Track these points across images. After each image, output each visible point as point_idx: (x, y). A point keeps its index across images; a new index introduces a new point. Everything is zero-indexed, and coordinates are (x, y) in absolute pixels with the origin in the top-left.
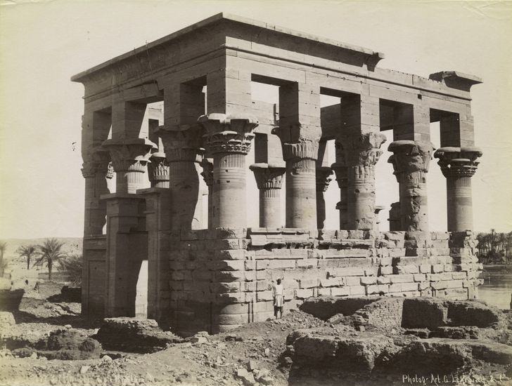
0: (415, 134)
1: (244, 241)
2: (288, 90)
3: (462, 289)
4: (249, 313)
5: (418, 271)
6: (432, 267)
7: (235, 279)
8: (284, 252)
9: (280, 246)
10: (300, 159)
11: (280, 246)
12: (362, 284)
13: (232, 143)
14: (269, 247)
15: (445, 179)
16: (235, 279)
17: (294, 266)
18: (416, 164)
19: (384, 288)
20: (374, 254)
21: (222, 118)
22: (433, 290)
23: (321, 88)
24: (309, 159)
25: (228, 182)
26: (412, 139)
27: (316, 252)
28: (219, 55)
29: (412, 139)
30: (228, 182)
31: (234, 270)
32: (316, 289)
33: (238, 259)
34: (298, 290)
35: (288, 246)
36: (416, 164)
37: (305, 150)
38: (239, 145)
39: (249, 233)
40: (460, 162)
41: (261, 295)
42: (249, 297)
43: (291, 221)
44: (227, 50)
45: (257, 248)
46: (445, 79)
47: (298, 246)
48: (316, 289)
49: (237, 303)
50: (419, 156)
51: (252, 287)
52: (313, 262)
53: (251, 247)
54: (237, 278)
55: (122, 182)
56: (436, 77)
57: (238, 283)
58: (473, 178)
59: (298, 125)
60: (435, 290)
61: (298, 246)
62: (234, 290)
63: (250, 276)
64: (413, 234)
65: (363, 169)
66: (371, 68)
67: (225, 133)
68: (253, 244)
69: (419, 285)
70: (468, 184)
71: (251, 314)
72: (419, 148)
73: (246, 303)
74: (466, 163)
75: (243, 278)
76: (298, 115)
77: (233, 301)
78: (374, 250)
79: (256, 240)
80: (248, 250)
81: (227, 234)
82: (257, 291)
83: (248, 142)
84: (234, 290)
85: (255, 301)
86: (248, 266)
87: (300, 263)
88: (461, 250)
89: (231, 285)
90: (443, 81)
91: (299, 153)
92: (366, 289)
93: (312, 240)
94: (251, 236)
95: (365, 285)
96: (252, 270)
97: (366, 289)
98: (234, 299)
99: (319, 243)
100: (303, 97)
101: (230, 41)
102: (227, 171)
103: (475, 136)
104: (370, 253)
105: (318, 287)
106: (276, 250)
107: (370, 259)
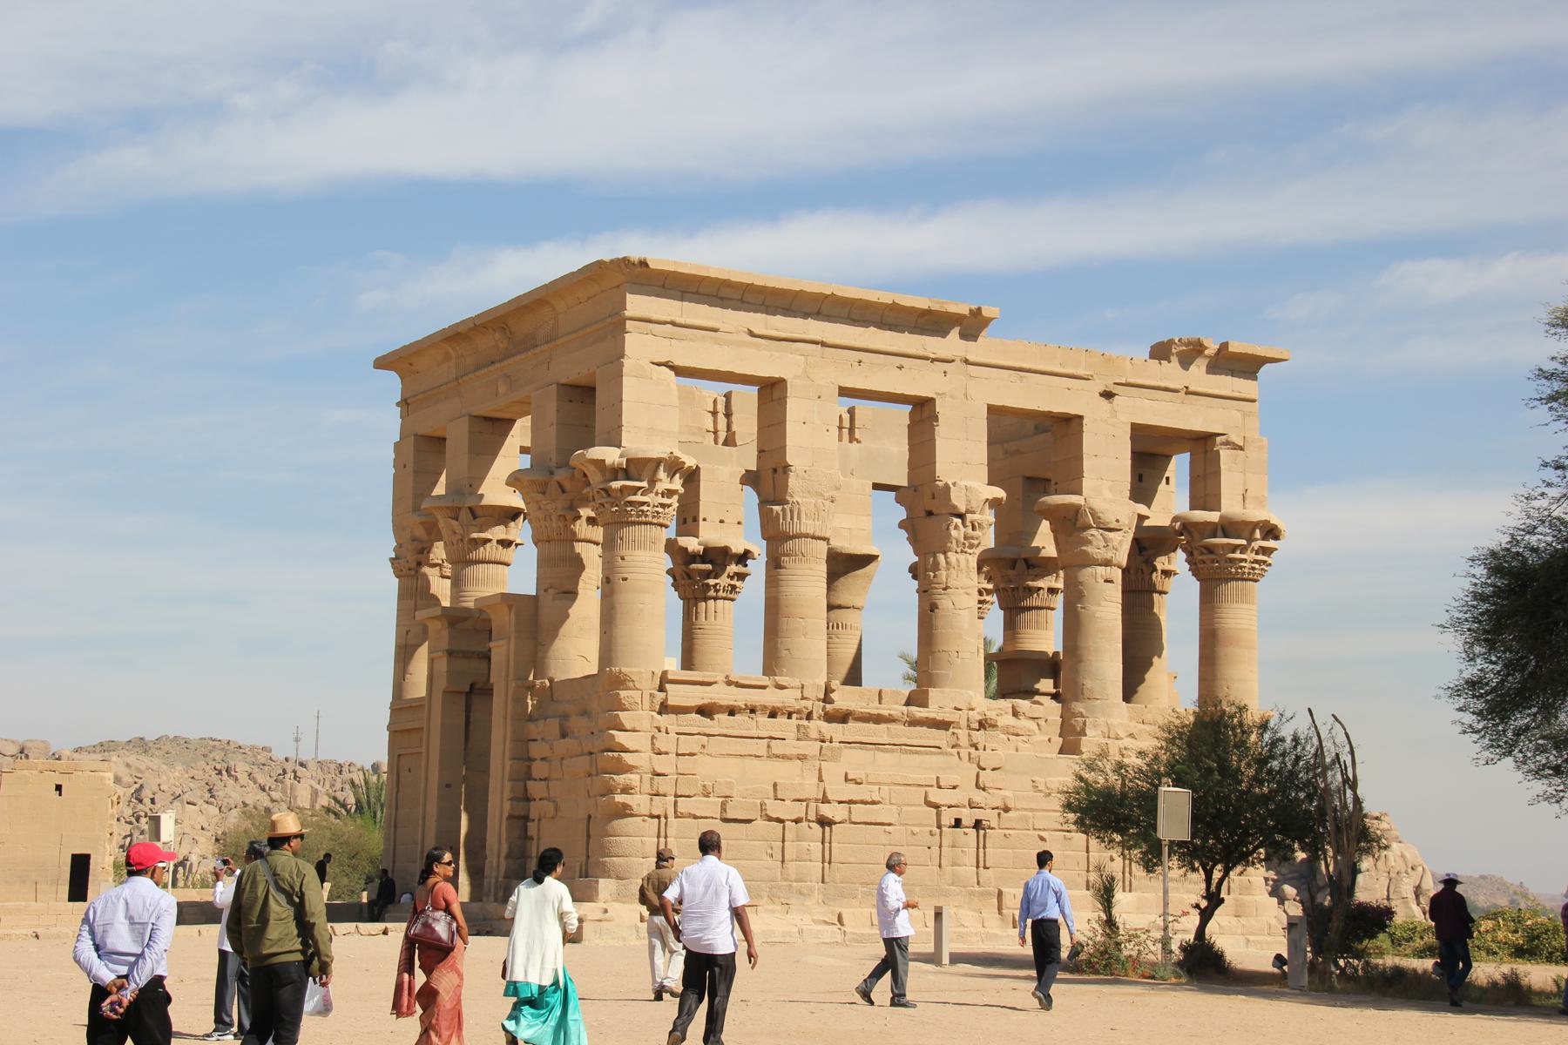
0: (1085, 482)
2: (772, 391)
7: (629, 769)
10: (790, 537)
12: (928, 804)
13: (631, 503)
14: (705, 711)
16: (629, 769)
17: (763, 751)
18: (1089, 549)
19: (988, 816)
20: (964, 741)
21: (611, 455)
23: (841, 388)
24: (807, 536)
26: (1079, 492)
27: (818, 726)
28: (616, 326)
29: (1079, 492)
32: (813, 805)
33: (638, 730)
34: (770, 803)
37: (799, 518)
38: (645, 508)
39: (664, 681)
40: (1216, 545)
42: (662, 805)
43: (772, 662)
45: (681, 710)
46: (1178, 354)
47: (773, 715)
49: (632, 815)
50: (1093, 531)
51: (664, 785)
52: (811, 748)
53: (664, 709)
55: (457, 583)
57: (637, 777)
59: (786, 468)
62: (626, 790)
63: (661, 764)
64: (1078, 707)
65: (941, 557)
67: (616, 485)
71: (662, 840)
73: (652, 816)
74: (1234, 548)
76: (784, 447)
77: (624, 812)
78: (962, 733)
79: (677, 695)
80: (660, 713)
81: (620, 682)
83: (666, 501)
84: (626, 790)
86: (659, 745)
87: (777, 747)
89: (621, 779)
90: (1174, 359)
91: (785, 525)
92: (939, 816)
93: (808, 704)
94: (668, 686)
95: (937, 807)
97: (939, 816)
98: (626, 806)
101: (636, 304)
105: (817, 800)
106: (722, 717)
107: (954, 751)
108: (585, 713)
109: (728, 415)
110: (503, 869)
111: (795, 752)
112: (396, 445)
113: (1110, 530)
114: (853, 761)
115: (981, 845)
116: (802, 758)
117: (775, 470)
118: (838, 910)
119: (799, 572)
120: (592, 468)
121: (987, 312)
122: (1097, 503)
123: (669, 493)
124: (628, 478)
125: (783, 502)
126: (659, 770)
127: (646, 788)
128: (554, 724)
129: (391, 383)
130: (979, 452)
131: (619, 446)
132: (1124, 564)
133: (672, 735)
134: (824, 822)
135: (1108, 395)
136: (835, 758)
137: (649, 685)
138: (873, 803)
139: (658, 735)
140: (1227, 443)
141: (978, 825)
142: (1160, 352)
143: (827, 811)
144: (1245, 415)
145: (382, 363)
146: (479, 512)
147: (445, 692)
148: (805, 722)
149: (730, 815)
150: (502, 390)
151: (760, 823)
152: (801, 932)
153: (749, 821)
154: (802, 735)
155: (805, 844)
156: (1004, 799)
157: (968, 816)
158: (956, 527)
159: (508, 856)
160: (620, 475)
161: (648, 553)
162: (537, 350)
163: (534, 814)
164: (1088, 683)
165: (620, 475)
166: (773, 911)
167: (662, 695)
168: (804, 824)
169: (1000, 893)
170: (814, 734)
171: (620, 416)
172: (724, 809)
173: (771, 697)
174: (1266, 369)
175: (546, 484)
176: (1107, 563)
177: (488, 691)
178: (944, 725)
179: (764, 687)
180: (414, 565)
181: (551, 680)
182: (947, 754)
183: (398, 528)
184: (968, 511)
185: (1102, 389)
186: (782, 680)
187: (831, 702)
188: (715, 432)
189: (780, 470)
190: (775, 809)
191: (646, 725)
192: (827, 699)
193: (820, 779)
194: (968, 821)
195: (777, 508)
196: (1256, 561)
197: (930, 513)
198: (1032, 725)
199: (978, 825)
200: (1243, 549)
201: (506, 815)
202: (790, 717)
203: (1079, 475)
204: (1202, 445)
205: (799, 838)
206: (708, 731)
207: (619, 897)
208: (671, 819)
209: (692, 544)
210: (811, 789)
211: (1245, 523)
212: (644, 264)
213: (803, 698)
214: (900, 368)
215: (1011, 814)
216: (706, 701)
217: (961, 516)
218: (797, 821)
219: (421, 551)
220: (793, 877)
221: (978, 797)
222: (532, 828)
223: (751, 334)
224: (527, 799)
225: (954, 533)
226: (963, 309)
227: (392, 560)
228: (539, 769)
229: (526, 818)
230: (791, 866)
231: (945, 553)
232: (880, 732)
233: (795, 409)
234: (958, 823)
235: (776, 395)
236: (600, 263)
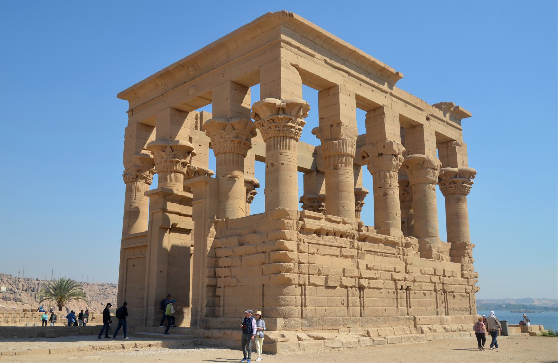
0: (426, 150)
1: (297, 223)
3: (464, 294)
4: (301, 295)
5: (433, 273)
6: (444, 271)
7: (290, 260)
8: (330, 240)
14: (318, 232)
15: (444, 198)
16: (290, 260)
18: (428, 176)
19: (410, 284)
20: (401, 252)
21: (278, 102)
22: (445, 292)
25: (283, 164)
28: (276, 46)
30: (283, 164)
31: (288, 250)
33: (292, 241)
35: (335, 234)
36: (428, 176)
37: (346, 146)
38: (293, 130)
41: (314, 279)
42: (304, 279)
44: (282, 44)
47: (341, 236)
48: (357, 279)
52: (355, 252)
53: (303, 230)
54: (292, 259)
56: (438, 106)
58: (468, 197)
59: (339, 124)
60: (446, 292)
62: (289, 270)
63: (304, 258)
66: (391, 86)
68: (307, 226)
69: (435, 286)
70: (465, 201)
71: (303, 297)
72: (430, 161)
76: (339, 114)
77: (289, 282)
78: (401, 248)
80: (300, 232)
82: (309, 275)
84: (289, 270)
87: (345, 252)
88: (463, 259)
89: (285, 265)
93: (353, 231)
94: (305, 219)
95: (395, 280)
96: (304, 252)
99: (359, 234)
100: (343, 98)
101: (283, 37)
102: (281, 154)
103: (464, 161)
105: (357, 277)
108: (255, 232)
111: (349, 254)
112: (127, 130)
115: (408, 297)
116: (352, 257)
117: (331, 126)
118: (367, 329)
119: (346, 171)
120: (265, 109)
121: (401, 74)
124: (284, 113)
125: (337, 139)
126: (302, 261)
127: (296, 270)
128: (234, 240)
129: (125, 105)
130: (398, 131)
131: (280, 98)
133: (306, 243)
134: (361, 288)
136: (363, 258)
137: (295, 217)
138: (376, 279)
139: (300, 243)
141: (408, 289)
142: (438, 106)
143: (364, 282)
144: (460, 135)
145: (122, 95)
146: (174, 148)
148: (352, 240)
149: (330, 284)
150: (191, 92)
151: (338, 288)
152: (359, 341)
153: (334, 288)
154: (352, 247)
155: (355, 298)
156: (414, 277)
157: (405, 285)
158: (394, 160)
159: (206, 306)
160: (281, 112)
161: (293, 152)
162: (215, 70)
164: (430, 230)
165: (281, 112)
166: (345, 331)
167: (301, 223)
169: (415, 319)
170: (356, 246)
171: (279, 85)
172: (326, 280)
173: (341, 227)
174: (463, 121)
175: (226, 125)
178: (394, 244)
179: (338, 222)
180: (135, 177)
181: (227, 219)
182: (396, 257)
183: (126, 163)
186: (346, 219)
187: (362, 231)
189: (335, 126)
190: (347, 282)
191: (295, 237)
192: (359, 230)
193: (358, 267)
194: (405, 287)
195: (336, 142)
197: (381, 155)
199: (408, 289)
201: (206, 285)
203: (423, 147)
207: (287, 327)
208: (307, 286)
210: (356, 274)
212: (291, 15)
215: (416, 284)
216: (319, 227)
217: (396, 156)
218: (351, 287)
219: (139, 171)
220: (351, 314)
221: (407, 276)
222: (219, 292)
223: (326, 62)
224: (215, 276)
225: (394, 162)
226: (394, 71)
227: (124, 176)
228: (221, 262)
230: (351, 308)
231: (389, 172)
232: (376, 247)
235: (331, 92)
236: (268, 15)
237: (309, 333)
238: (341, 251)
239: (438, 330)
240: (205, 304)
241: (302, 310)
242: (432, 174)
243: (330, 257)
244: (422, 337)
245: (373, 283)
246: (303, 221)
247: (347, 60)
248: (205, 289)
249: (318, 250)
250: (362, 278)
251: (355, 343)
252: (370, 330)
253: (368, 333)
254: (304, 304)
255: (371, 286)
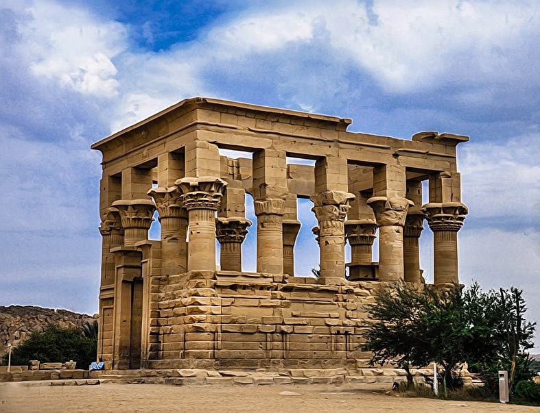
0: (388, 192)
9: (244, 287)
11: (244, 287)
14: (234, 287)
21: (193, 181)
26: (386, 196)
27: (279, 293)
31: (200, 305)
47: (262, 288)
52: (278, 302)
61: (262, 288)
62: (200, 321)
63: (216, 310)
65: (329, 223)
67: (194, 193)
74: (447, 218)
75: (209, 312)
85: (219, 330)
87: (263, 303)
89: (198, 316)
104: (335, 298)
109: (238, 167)
110: (148, 355)
113: (398, 211)
114: (296, 309)
122: (392, 200)
123: (216, 197)
126: (214, 313)
130: (344, 179)
132: (404, 224)
134: (283, 333)
135: (396, 156)
140: (445, 175)
145: (95, 147)
147: (124, 282)
149: (244, 331)
156: (357, 322)
159: (150, 351)
163: (161, 332)
166: (262, 371)
167: (215, 281)
168: (275, 335)
176: (397, 224)
177: (141, 282)
184: (341, 203)
185: (394, 153)
187: (285, 283)
188: (233, 175)
189: (262, 186)
191: (209, 294)
196: (457, 223)
198: (367, 292)
199: (346, 333)
200: (452, 218)
201: (149, 333)
202: (268, 290)
204: (433, 176)
205: (273, 340)
206: (234, 296)
209: (224, 220)
211: (452, 208)
213: (274, 282)
214: (312, 144)
217: (338, 205)
221: (347, 321)
229: (158, 334)
233: (268, 161)
234: (338, 333)
237: (221, 372)
238: (260, 302)
239: (385, 374)
240: (148, 349)
241: (214, 352)
242: (395, 216)
243: (248, 308)
244: (360, 379)
245: (298, 329)
246: (216, 279)
247: (277, 122)
248: (149, 336)
249: (232, 303)
250: (285, 325)
251: (269, 380)
252: (291, 370)
253: (290, 372)
254: (216, 347)
255: (296, 331)
